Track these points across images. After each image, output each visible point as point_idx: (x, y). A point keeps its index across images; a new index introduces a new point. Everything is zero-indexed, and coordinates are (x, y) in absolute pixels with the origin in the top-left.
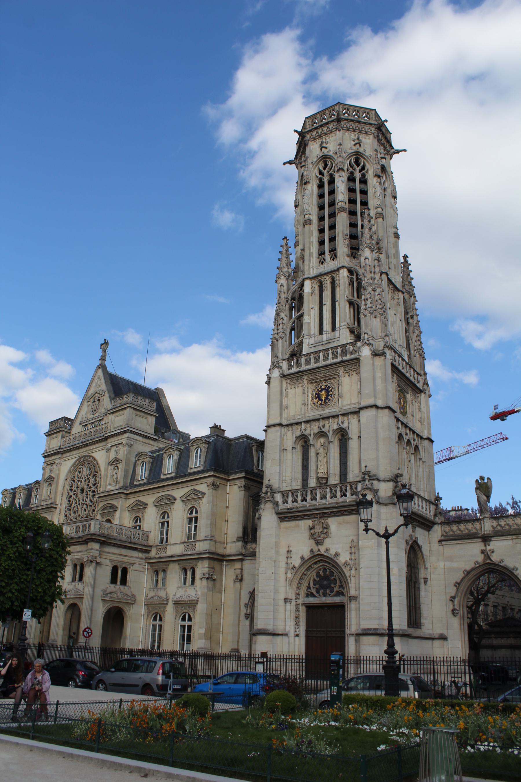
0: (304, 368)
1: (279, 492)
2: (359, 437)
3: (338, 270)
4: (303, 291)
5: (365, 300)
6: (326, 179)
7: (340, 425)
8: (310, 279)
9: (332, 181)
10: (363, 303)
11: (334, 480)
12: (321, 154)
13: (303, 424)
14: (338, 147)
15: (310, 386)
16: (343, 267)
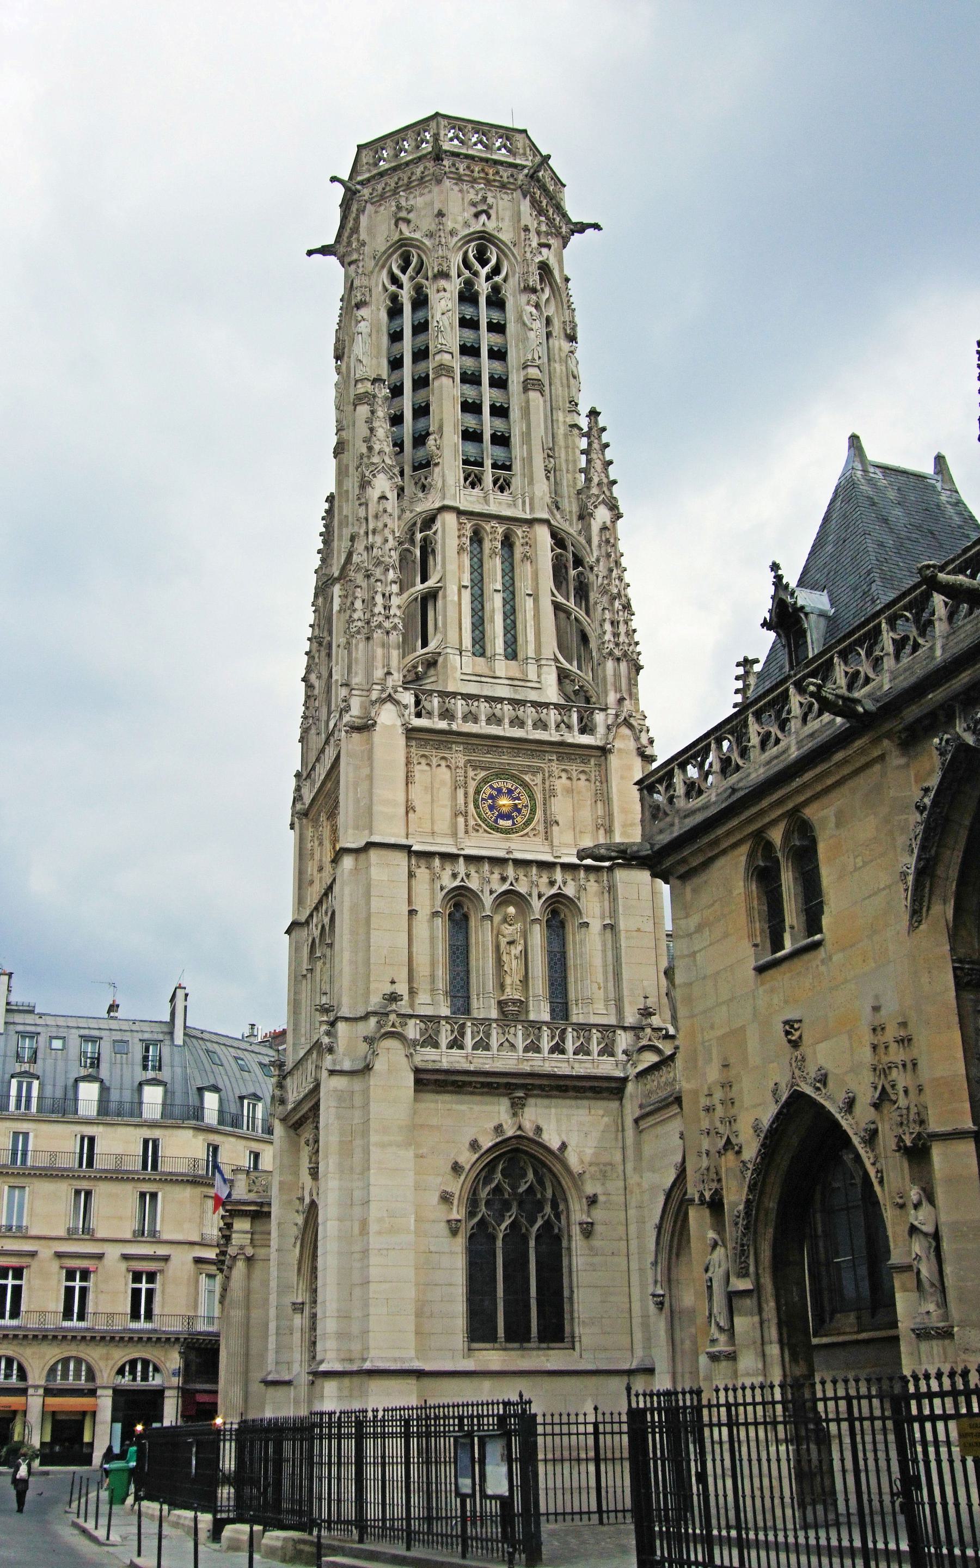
0: (458, 725)
1: (411, 1016)
2: (611, 928)
3: (531, 522)
4: (435, 533)
5: (612, 623)
6: (483, 288)
7: (560, 888)
8: (459, 512)
9: (496, 302)
10: (608, 627)
11: (541, 1011)
12: (476, 226)
13: (461, 860)
14: (523, 234)
15: (471, 773)
16: (547, 522)
